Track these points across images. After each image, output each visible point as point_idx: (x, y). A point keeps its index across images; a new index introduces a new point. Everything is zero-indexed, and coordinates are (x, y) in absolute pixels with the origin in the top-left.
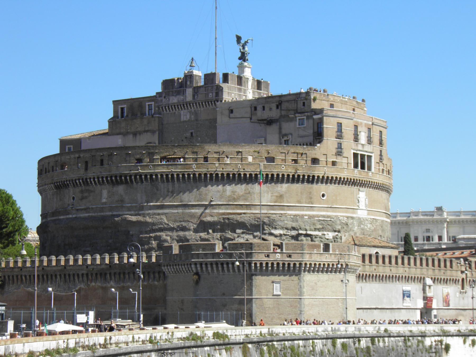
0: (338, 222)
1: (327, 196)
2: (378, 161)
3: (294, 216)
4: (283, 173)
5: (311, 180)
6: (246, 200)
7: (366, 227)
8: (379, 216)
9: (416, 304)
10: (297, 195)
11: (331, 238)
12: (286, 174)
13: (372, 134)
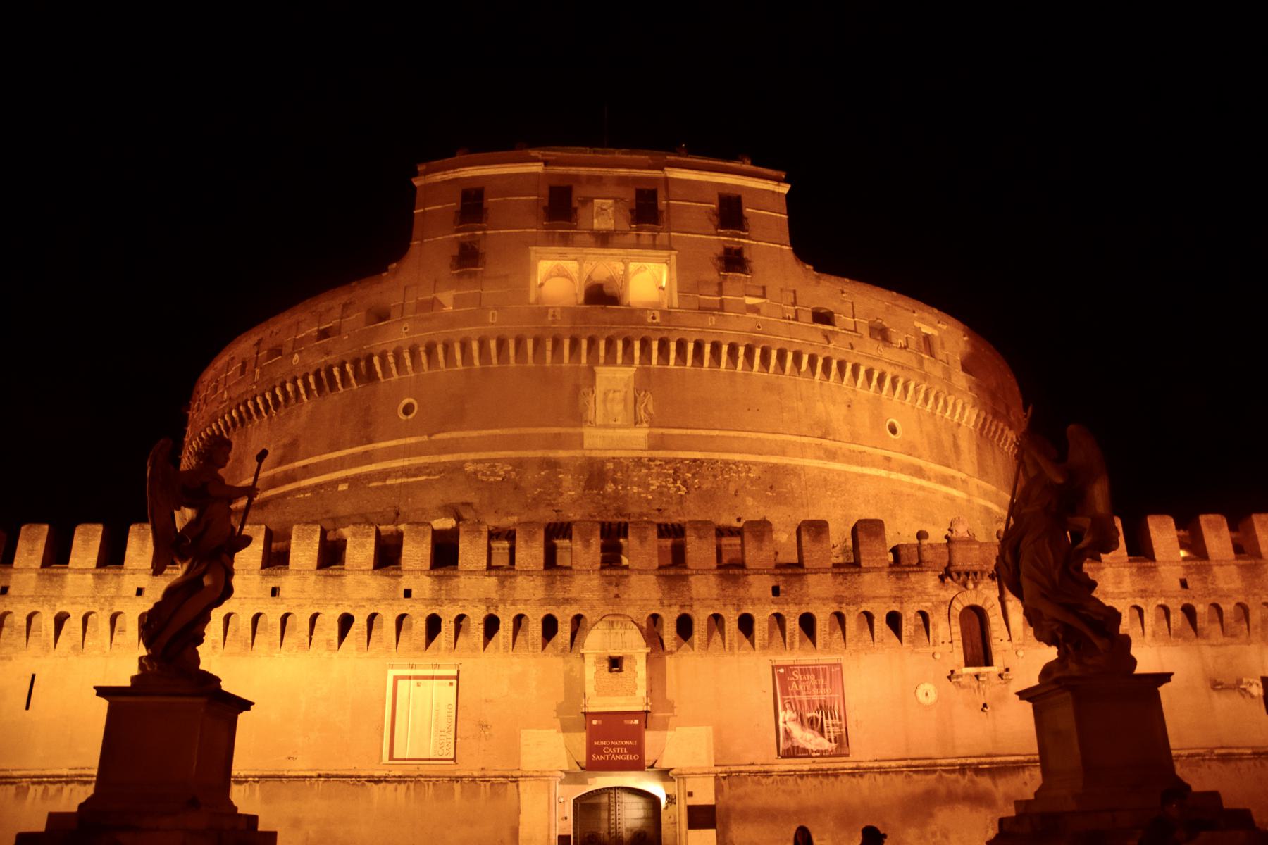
7: (635, 489)
9: (513, 750)
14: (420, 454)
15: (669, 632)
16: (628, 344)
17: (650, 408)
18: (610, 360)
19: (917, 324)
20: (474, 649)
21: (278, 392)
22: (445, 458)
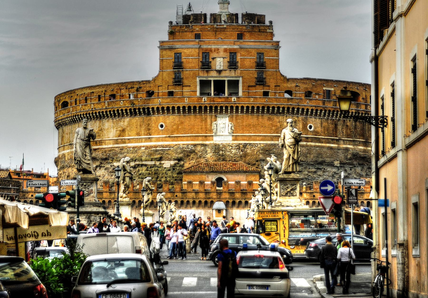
0: (179, 151)
1: (166, 126)
2: (254, 84)
3: (133, 148)
4: (122, 108)
5: (147, 112)
6: (99, 136)
7: (228, 153)
8: (261, 140)
10: (137, 128)
11: (169, 166)
12: (124, 109)
13: (239, 57)
14: (166, 141)
15: (230, 205)
16: (227, 107)
17: (233, 128)
18: (221, 112)
19: (324, 88)
20: (191, 207)
21: (116, 112)
22: (175, 143)
